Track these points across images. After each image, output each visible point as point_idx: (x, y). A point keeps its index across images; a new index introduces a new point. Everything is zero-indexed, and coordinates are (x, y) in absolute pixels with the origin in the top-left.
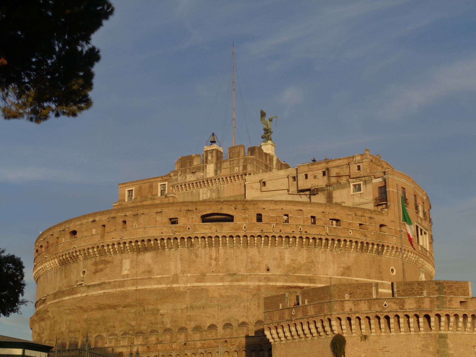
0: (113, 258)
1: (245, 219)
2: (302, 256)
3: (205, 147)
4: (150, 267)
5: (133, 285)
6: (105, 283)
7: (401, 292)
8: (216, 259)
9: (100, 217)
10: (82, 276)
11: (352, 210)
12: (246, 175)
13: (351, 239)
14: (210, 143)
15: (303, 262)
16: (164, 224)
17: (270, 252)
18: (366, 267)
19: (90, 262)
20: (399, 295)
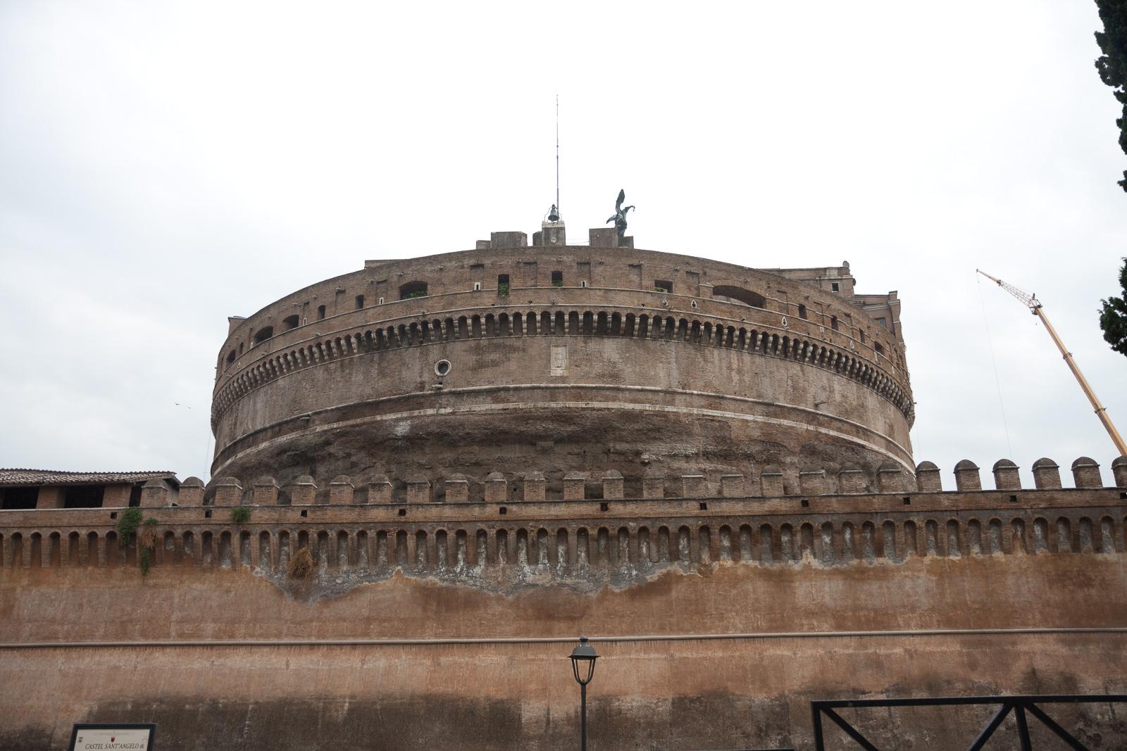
0: (524, 341)
4: (614, 367)
5: (578, 398)
6: (507, 389)
8: (739, 372)
9: (494, 258)
16: (647, 288)
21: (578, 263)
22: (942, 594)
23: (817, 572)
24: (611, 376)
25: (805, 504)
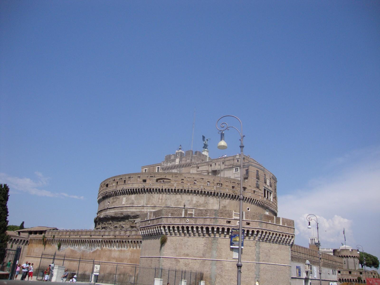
1: (176, 181)
2: (201, 199)
3: (176, 151)
4: (133, 201)
5: (126, 209)
6: (115, 207)
7: (196, 215)
8: (161, 199)
10: (108, 204)
11: (229, 179)
12: (191, 163)
13: (227, 193)
14: (179, 149)
15: (202, 203)
17: (187, 197)
18: (234, 207)
19: (111, 198)
20: (195, 216)
21: (129, 178)
22: (131, 256)
23: (116, 250)
24: (132, 203)
25: (115, 236)
